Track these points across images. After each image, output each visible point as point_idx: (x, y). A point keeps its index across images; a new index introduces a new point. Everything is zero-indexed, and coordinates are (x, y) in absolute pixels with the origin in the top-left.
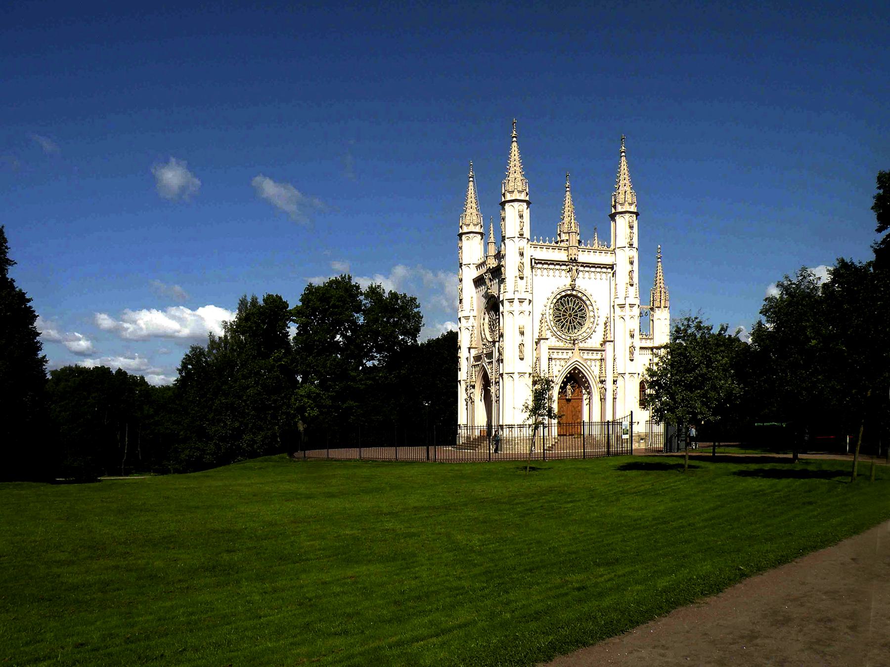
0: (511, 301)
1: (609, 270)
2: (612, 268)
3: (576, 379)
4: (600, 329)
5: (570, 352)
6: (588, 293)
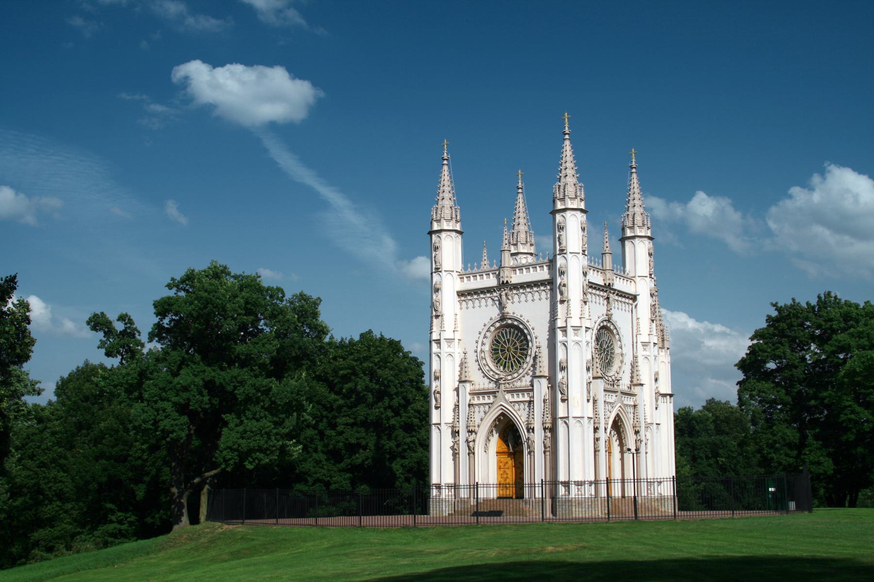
0: (576, 329)
1: (631, 302)
2: (634, 298)
3: (617, 425)
4: (627, 368)
5: (614, 395)
6: (619, 324)
